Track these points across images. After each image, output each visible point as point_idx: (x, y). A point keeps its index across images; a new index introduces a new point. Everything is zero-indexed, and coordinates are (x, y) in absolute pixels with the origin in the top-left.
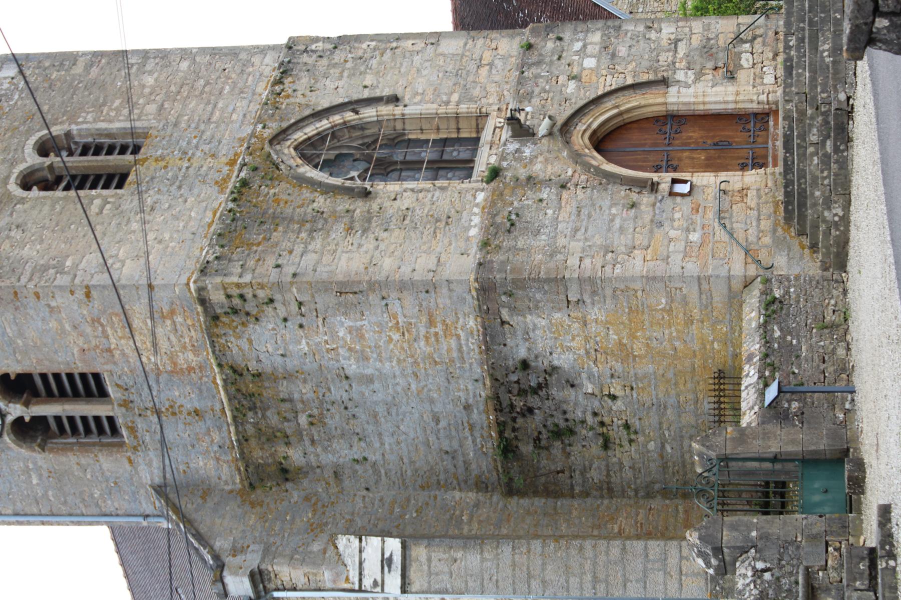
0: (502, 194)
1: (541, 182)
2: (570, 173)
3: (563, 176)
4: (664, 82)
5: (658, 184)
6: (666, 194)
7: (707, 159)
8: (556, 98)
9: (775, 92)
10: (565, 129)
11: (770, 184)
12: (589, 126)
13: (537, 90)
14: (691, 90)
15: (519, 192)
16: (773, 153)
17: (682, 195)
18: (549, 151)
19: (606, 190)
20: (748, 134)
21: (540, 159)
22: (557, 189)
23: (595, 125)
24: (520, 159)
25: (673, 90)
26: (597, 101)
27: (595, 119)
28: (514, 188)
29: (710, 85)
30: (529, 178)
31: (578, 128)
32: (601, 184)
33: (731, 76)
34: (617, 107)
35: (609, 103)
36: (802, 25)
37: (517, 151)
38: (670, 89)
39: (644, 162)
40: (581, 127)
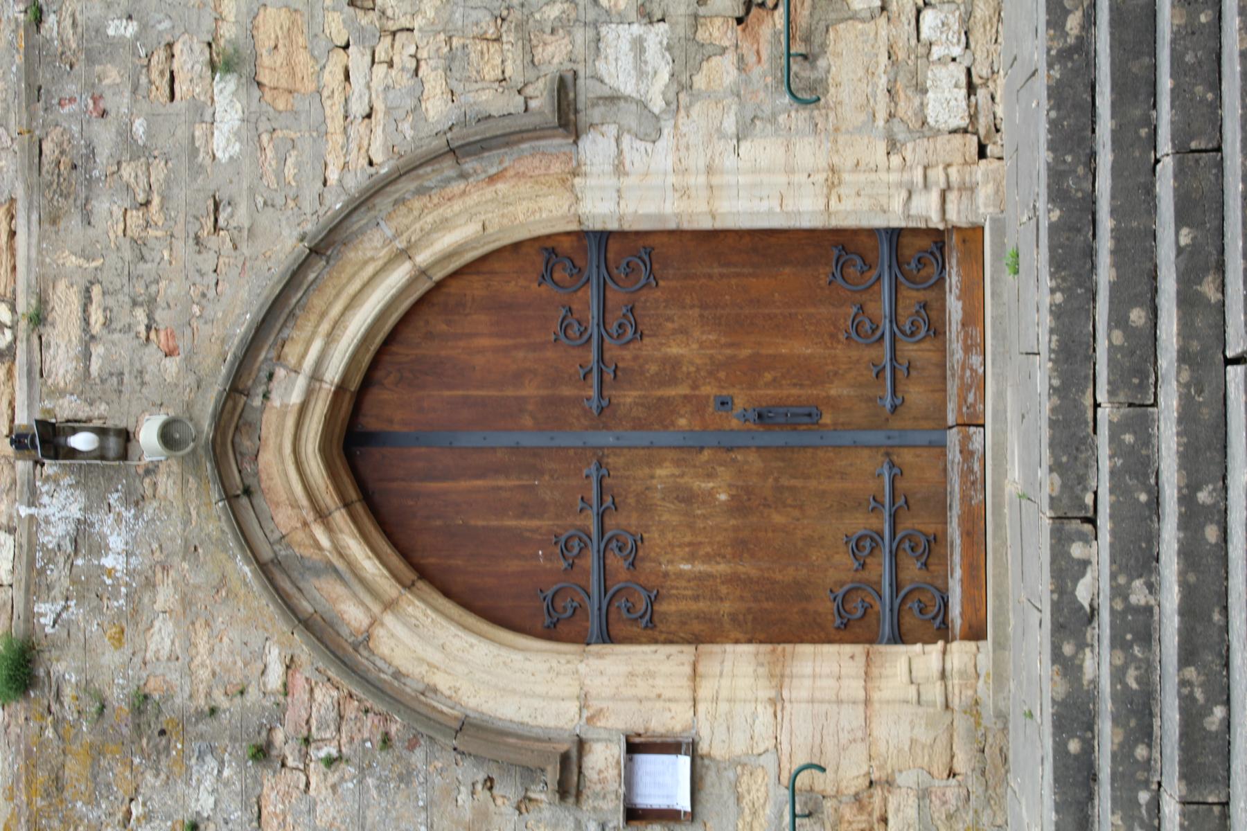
0: (58, 783)
1: (183, 723)
2: (275, 678)
3: (253, 694)
4: (567, 113)
5: (581, 744)
6: (614, 812)
7: (739, 506)
8: (181, 195)
9: (969, 189)
10: (223, 446)
11: (960, 765)
12: (316, 377)
13: (105, 137)
14: (663, 155)
15: (116, 773)
16: (966, 499)
17: (669, 815)
18: (190, 551)
19: (405, 778)
20: (870, 353)
21: (165, 596)
22: (242, 766)
23: (333, 373)
24: (88, 588)
25: (596, 148)
26: (326, 246)
27: (331, 338)
28: (96, 752)
29: (730, 125)
30: (141, 701)
31: (276, 401)
32: (386, 741)
33: (800, 81)
34: (405, 254)
35: (372, 245)
36: (1139, 596)
37: (83, 538)
38: (586, 143)
39: (524, 511)
40: (288, 392)
